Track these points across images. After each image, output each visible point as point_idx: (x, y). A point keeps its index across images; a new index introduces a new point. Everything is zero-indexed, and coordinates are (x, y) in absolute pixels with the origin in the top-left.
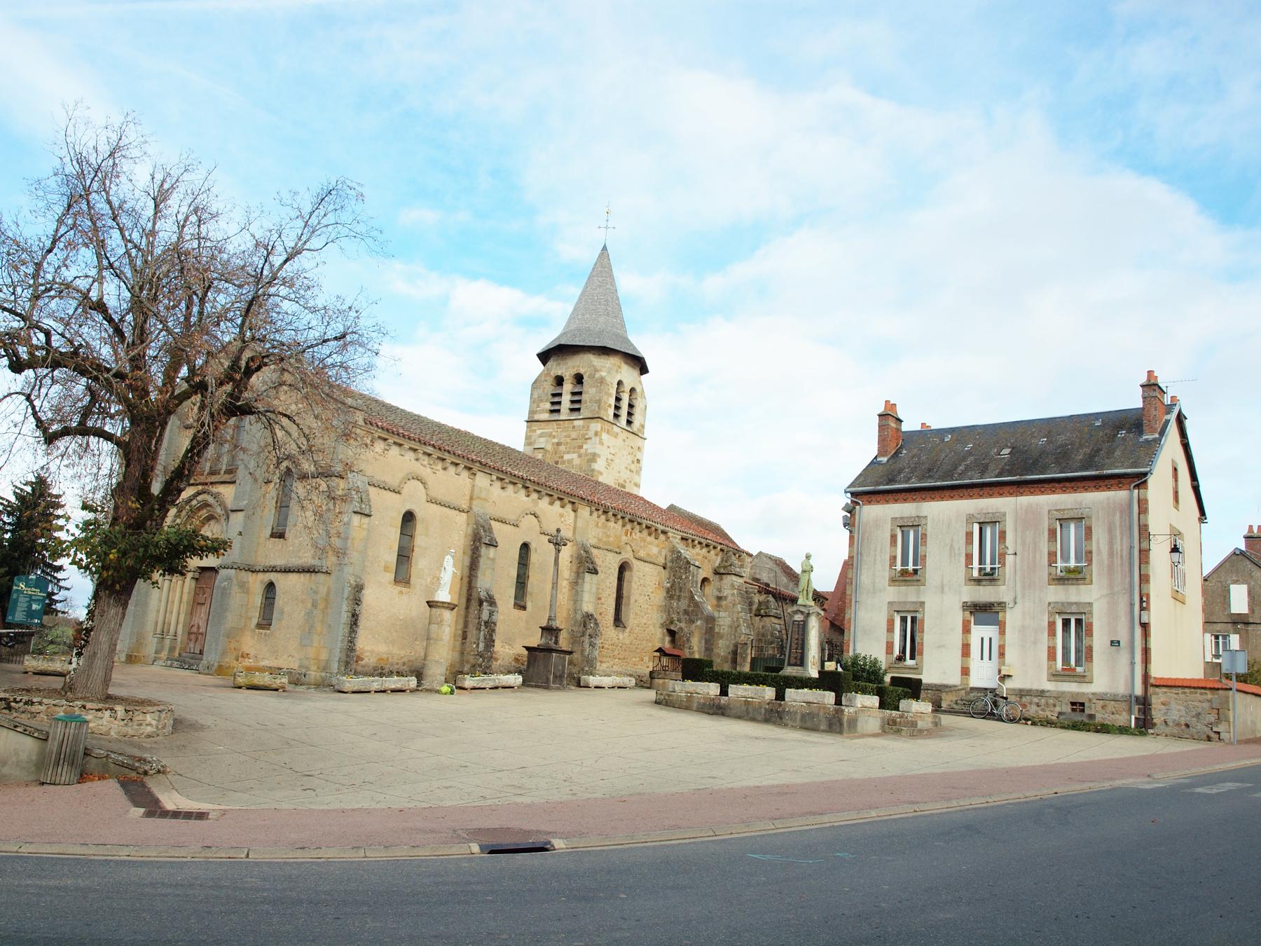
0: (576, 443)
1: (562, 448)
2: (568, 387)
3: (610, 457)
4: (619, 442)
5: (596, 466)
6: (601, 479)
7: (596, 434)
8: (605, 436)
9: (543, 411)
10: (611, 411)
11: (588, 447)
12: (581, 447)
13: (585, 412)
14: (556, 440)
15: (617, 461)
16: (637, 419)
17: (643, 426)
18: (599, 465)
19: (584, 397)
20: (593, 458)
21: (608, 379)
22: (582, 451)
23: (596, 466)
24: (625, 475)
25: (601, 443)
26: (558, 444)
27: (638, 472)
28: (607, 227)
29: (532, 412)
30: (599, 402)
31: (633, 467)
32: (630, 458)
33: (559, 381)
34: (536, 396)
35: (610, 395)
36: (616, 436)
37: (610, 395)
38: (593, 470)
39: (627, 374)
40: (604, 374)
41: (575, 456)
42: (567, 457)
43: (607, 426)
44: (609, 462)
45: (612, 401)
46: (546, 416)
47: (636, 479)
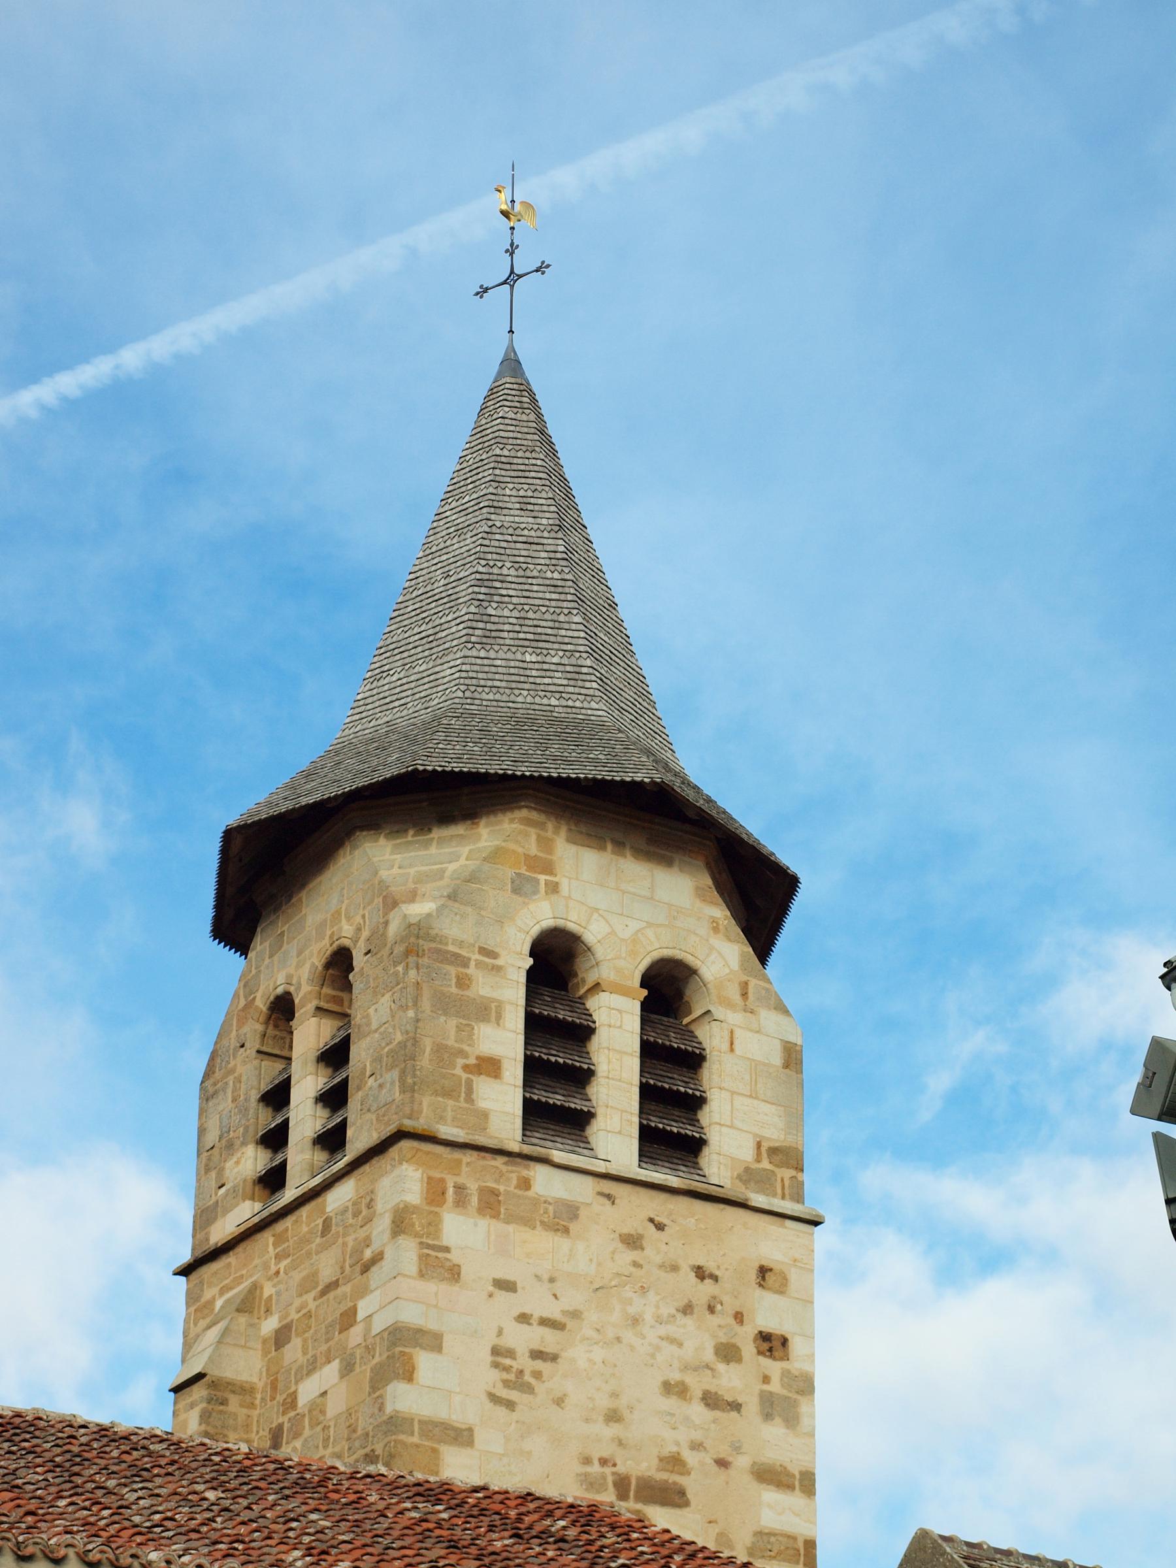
0: (331, 1309)
1: (293, 1352)
2: (310, 1034)
3: (522, 1339)
4: (591, 1250)
5: (403, 1398)
6: (460, 1468)
7: (400, 1224)
8: (461, 1230)
9: (237, 1195)
10: (502, 1103)
11: (379, 1309)
12: (348, 1318)
13: (359, 1140)
14: (270, 1325)
15: (580, 1353)
16: (733, 1125)
17: (788, 1157)
18: (441, 1388)
19: (359, 1053)
20: (400, 1351)
21: (457, 930)
22: (355, 1335)
23: (403, 1398)
24: (658, 1431)
25: (439, 1265)
26: (281, 1338)
27: (788, 1403)
28: (512, 279)
29: (204, 1217)
30: (404, 1056)
31: (732, 1380)
32: (698, 1339)
33: (283, 1009)
34: (212, 1137)
35: (487, 1011)
36: (562, 1220)
37: (487, 1011)
38: (396, 1423)
39: (634, 910)
40: (418, 910)
41: (329, 1373)
42: (307, 1391)
43: (472, 1173)
44: (516, 1377)
45: (506, 1040)
46: (246, 1211)
47: (773, 1442)
